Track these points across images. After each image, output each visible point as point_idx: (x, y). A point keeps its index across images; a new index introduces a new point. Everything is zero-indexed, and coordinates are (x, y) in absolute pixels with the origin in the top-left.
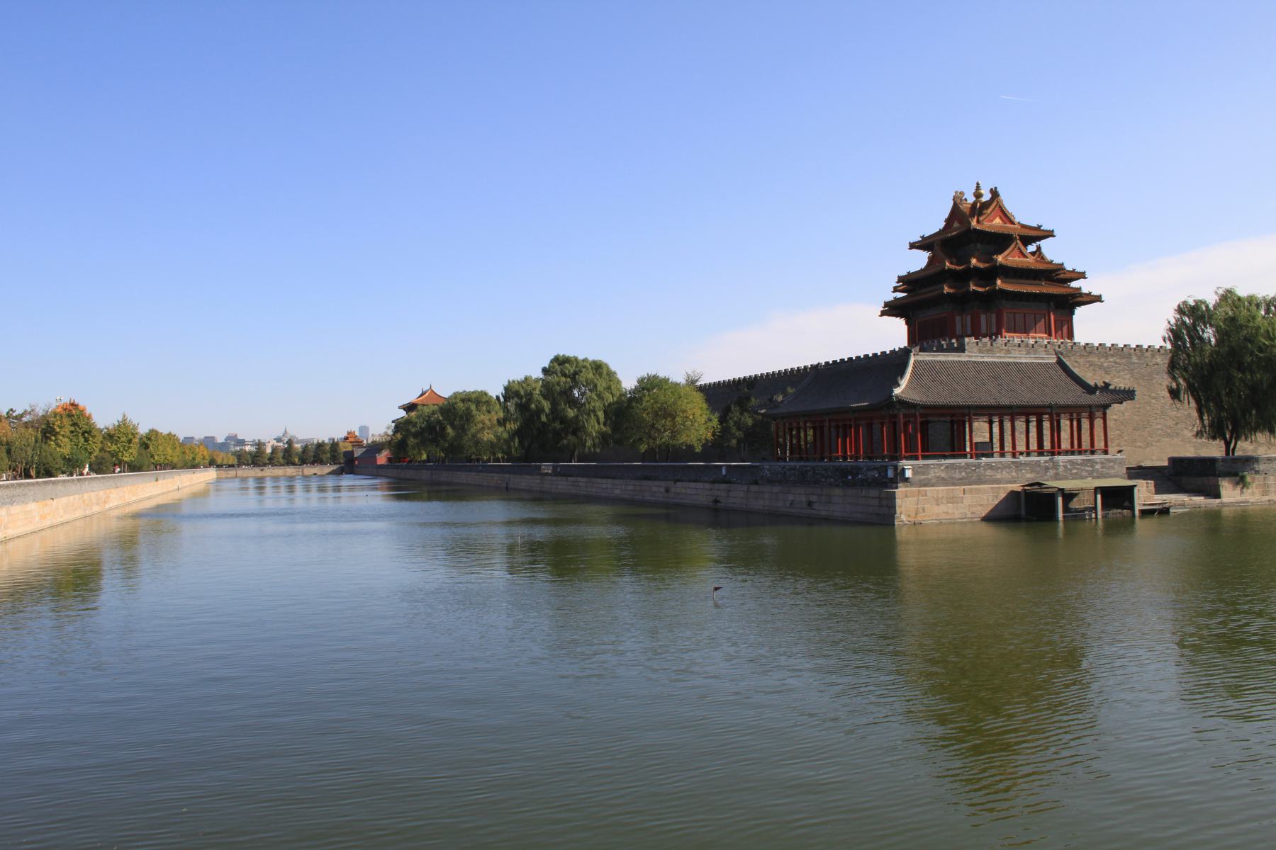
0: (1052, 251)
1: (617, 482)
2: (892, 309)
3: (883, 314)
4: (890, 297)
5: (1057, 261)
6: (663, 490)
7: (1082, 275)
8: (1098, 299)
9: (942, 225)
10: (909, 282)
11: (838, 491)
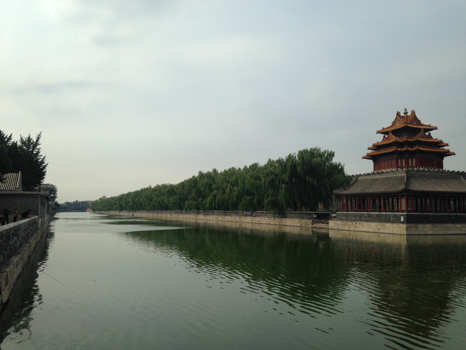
0: (434, 135)
2: (369, 157)
3: (363, 158)
4: (370, 151)
5: (439, 139)
7: (447, 145)
8: (454, 154)
9: (390, 124)
10: (377, 147)
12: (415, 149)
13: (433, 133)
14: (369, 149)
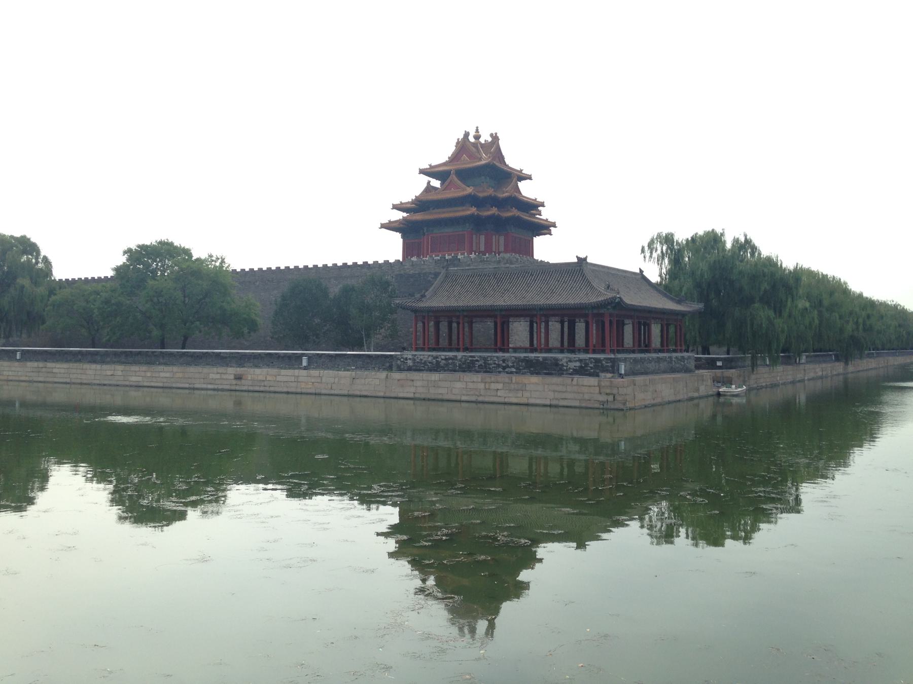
0: (527, 190)
1: (135, 368)
3: (383, 226)
5: (539, 200)
6: (232, 377)
10: (420, 205)
11: (535, 379)
12: (509, 214)
13: (523, 186)
14: (395, 207)
